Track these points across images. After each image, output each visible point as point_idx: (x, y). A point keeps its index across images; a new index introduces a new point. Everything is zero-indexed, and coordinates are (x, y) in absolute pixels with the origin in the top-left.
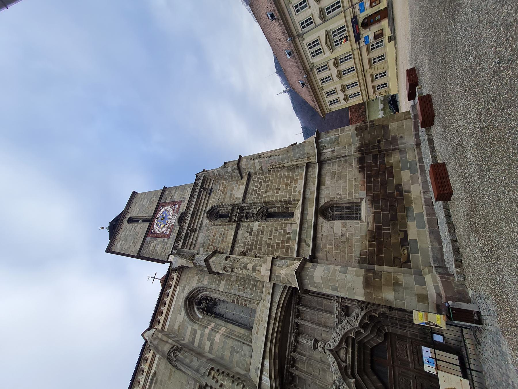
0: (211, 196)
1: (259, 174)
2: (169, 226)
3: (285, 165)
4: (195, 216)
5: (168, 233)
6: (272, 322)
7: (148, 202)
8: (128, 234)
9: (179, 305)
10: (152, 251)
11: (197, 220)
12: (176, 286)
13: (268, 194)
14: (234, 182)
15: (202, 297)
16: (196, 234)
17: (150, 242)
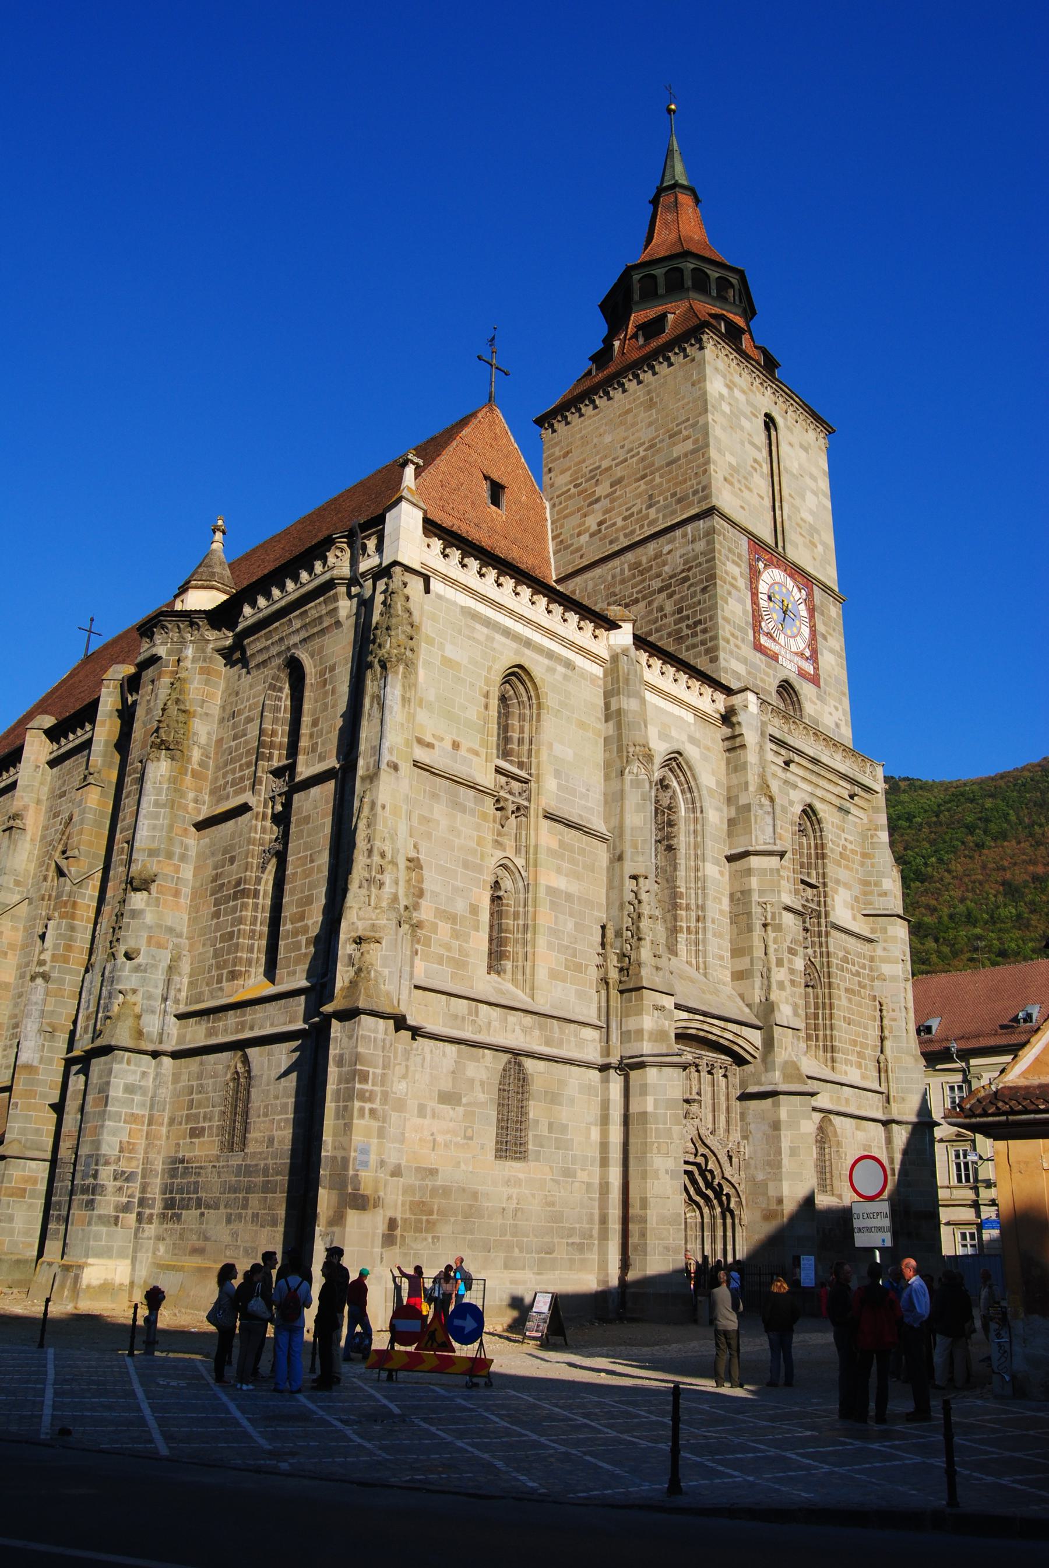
0: (835, 810)
1: (871, 969)
2: (774, 640)
3: (888, 1044)
4: (810, 766)
5: (764, 640)
6: (722, 1024)
7: (810, 519)
8: (742, 429)
9: (670, 727)
10: (727, 573)
11: (801, 772)
12: (695, 710)
13: (842, 993)
14: (857, 889)
15: (674, 792)
16: (779, 772)
17: (740, 556)
